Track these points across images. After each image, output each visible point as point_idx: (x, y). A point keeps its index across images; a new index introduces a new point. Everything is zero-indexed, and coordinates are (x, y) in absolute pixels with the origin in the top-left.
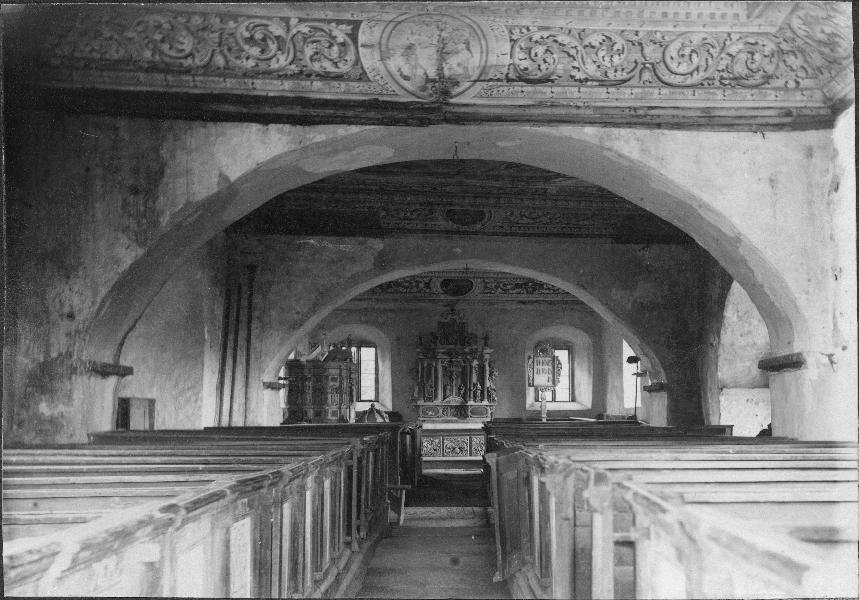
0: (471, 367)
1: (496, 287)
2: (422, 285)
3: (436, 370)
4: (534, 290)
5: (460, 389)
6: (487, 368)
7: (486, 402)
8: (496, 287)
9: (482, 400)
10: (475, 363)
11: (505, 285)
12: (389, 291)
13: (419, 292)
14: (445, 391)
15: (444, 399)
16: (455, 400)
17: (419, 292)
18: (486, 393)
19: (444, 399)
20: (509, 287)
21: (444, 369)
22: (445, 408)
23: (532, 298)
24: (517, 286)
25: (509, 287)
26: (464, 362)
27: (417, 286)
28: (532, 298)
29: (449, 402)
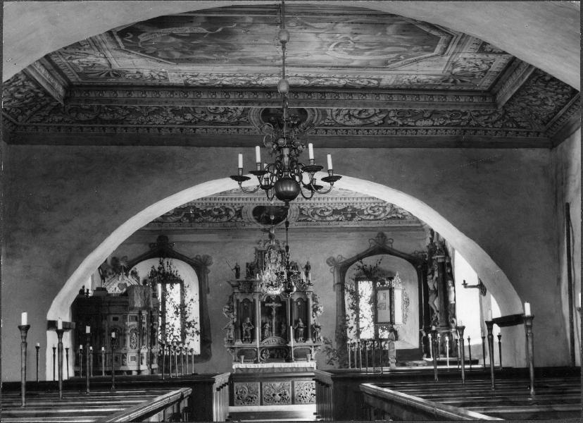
1: (313, 214)
2: (232, 214)
4: (353, 215)
6: (311, 303)
7: (310, 342)
8: (313, 214)
9: (306, 339)
11: (322, 211)
12: (197, 220)
14: (263, 330)
15: (263, 340)
16: (273, 341)
18: (310, 330)
19: (263, 340)
20: (327, 213)
21: (263, 304)
22: (263, 349)
23: (352, 224)
25: (327, 213)
27: (228, 215)
28: (352, 224)
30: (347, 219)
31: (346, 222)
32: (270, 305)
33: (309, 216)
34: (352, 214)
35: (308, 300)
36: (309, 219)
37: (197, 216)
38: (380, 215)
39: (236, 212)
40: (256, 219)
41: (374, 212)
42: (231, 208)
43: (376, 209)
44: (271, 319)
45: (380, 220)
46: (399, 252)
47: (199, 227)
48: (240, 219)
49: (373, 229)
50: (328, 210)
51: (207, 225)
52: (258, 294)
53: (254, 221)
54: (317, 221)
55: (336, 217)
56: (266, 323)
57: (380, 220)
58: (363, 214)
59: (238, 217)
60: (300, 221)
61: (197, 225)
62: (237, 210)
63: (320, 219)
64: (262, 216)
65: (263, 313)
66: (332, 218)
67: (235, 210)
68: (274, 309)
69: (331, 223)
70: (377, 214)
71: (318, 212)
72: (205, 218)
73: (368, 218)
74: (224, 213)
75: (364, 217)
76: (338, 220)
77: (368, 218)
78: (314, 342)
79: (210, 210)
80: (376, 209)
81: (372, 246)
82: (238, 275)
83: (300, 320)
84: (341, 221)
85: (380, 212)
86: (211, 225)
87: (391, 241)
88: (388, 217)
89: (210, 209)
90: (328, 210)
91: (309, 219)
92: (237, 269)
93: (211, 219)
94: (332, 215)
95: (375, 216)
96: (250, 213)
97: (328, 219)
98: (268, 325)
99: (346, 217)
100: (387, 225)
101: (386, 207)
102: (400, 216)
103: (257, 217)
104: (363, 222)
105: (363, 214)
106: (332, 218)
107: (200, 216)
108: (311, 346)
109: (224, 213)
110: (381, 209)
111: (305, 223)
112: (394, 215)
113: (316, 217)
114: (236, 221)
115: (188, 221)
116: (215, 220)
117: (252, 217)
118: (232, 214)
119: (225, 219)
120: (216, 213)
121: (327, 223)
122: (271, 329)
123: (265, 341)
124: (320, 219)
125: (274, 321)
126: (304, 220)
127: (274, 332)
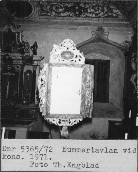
4: (80, 13)
8: (51, 10)
20: (61, 10)
23: (80, 20)
30: (76, 15)
31: (76, 18)
34: (78, 11)
36: (49, 14)
38: (99, 13)
41: (95, 11)
43: (97, 8)
45: (100, 17)
46: (113, 42)
49: (95, 25)
54: (54, 16)
55: (68, 13)
57: (100, 17)
58: (87, 12)
60: (42, 15)
63: (57, 15)
66: (65, 15)
69: (64, 18)
70: (97, 12)
71: (54, 8)
73: (91, 15)
75: (88, 15)
76: (69, 16)
77: (91, 15)
80: (97, 8)
81: (94, 36)
84: (72, 16)
85: (100, 11)
87: (107, 34)
88: (106, 15)
90: (61, 8)
91: (49, 14)
94: (65, 12)
95: (96, 14)
97: (62, 14)
99: (75, 13)
100: (105, 22)
101: (104, 7)
102: (114, 15)
104: (87, 18)
105: (87, 12)
106: (65, 15)
110: (100, 8)
111: (46, 17)
112: (110, 14)
113: (54, 13)
121: (62, 18)
124: (57, 15)
126: (45, 15)
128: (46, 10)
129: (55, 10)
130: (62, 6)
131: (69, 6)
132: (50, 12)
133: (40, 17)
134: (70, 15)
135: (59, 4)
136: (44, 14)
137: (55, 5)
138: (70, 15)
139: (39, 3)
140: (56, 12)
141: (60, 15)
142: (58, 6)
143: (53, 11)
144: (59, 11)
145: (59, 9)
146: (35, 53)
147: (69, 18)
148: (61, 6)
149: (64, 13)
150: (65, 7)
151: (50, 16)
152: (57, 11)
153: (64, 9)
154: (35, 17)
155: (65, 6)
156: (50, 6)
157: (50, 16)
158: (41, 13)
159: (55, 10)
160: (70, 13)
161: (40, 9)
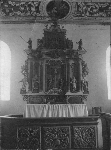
0: (68, 64)
1: (86, 11)
2: (33, 9)
3: (42, 68)
5: (60, 83)
6: (81, 67)
7: (80, 93)
8: (86, 11)
9: (77, 91)
10: (72, 62)
12: (10, 14)
13: (31, 15)
14: (48, 85)
16: (56, 91)
17: (31, 15)
20: (95, 11)
21: (48, 66)
24: (101, 10)
26: (64, 62)
27: (30, 10)
29: (51, 92)
31: (106, 18)
32: (53, 67)
33: (83, 13)
35: (79, 64)
36: (83, 15)
37: (10, 11)
39: (36, 7)
40: (48, 14)
42: (32, 4)
44: (54, 77)
47: (12, 19)
48: (38, 13)
50: (96, 8)
51: (17, 18)
52: (45, 60)
53: (47, 15)
55: (100, 14)
56: (50, 79)
59: (37, 13)
60: (77, 16)
61: (11, 18)
62: (36, 6)
63: (90, 15)
64: (53, 11)
65: (48, 73)
66: (98, 15)
67: (35, 5)
68: (56, 70)
71: (89, 9)
72: (16, 13)
74: (28, 9)
76: (101, 16)
78: (84, 93)
79: (18, 6)
82: (30, 47)
83: (74, 77)
84: (103, 17)
86: (20, 18)
89: (19, 5)
90: (96, 8)
91: (83, 15)
92: (30, 42)
93: (19, 13)
94: (98, 13)
96: (45, 9)
97: (95, 15)
98: (51, 81)
99: (106, 14)
103: (49, 13)
107: (13, 12)
108: (81, 96)
109: (28, 9)
111: (80, 18)
113: (88, 14)
114: (36, 16)
115: (5, 14)
116: (22, 14)
117: (46, 12)
118: (33, 9)
119: (29, 14)
120: (23, 9)
121: (94, 18)
122: (53, 83)
123: (50, 91)
124: (90, 15)
125: (55, 78)
127: (55, 86)
128: (82, 11)
129: (90, 11)
130: (97, 6)
131: (103, 7)
132: (85, 13)
133: (75, 19)
134: (102, 15)
135: (95, 4)
136: (79, 14)
137: (91, 5)
138: (102, 15)
139: (77, 4)
140: (90, 13)
141: (93, 16)
142: (93, 7)
143: (87, 12)
144: (93, 11)
145: (93, 10)
146: (80, 47)
147: (101, 18)
148: (96, 7)
149: (97, 14)
150: (100, 7)
151: (84, 17)
152: (92, 12)
153: (98, 9)
154: (70, 18)
155: (100, 6)
156: (86, 7)
157: (84, 17)
158: (76, 14)
159: (90, 11)
160: (102, 13)
161: (76, 10)
